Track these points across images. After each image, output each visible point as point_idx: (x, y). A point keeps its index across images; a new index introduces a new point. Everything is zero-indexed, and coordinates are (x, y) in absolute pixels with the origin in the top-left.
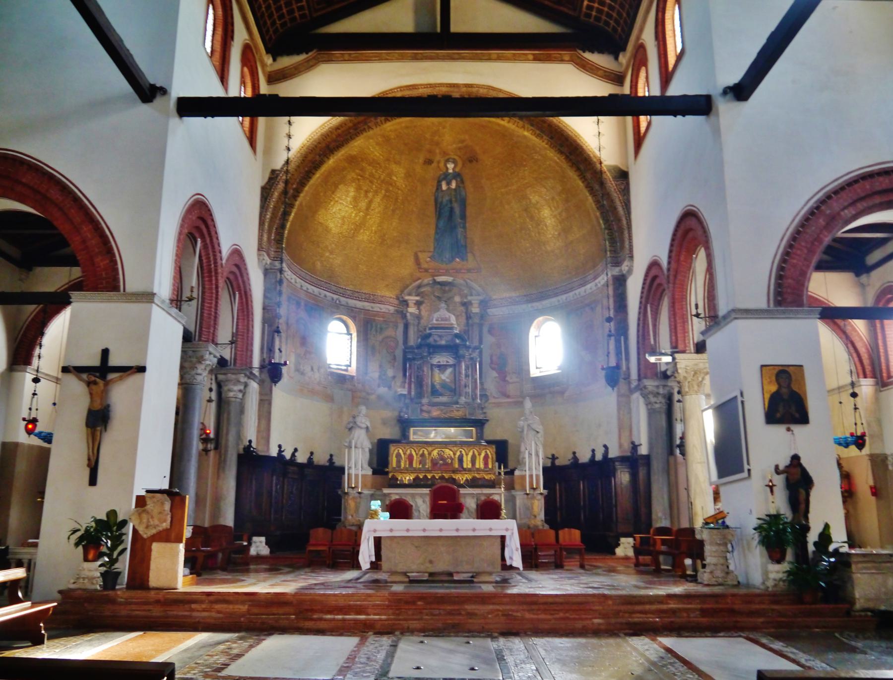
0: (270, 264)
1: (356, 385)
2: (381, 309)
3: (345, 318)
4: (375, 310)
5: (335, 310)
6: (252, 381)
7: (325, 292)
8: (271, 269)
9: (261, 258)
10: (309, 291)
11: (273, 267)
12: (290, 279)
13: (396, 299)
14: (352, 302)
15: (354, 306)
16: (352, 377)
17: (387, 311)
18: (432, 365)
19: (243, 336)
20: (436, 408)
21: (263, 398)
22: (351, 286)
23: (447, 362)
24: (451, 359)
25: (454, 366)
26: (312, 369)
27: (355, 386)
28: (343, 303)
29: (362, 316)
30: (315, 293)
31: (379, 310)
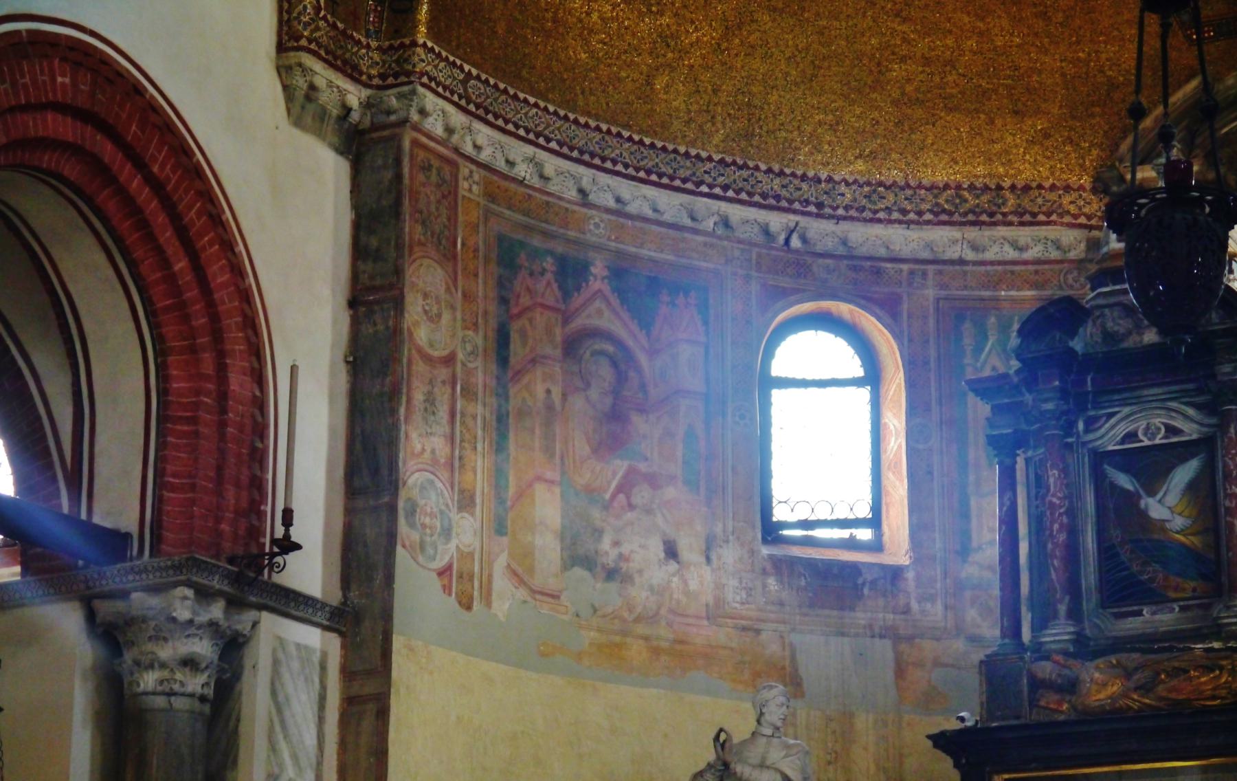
0: (367, 105)
1: (915, 606)
2: (1021, 249)
3: (844, 309)
4: (989, 255)
5: (785, 282)
6: (267, 618)
7: (723, 206)
8: (375, 127)
9: (300, 82)
10: (632, 209)
11: (382, 118)
12: (501, 165)
13: (1094, 191)
14: (865, 236)
15: (883, 252)
16: (895, 573)
17: (1054, 254)
18: (1100, 458)
19: (193, 420)
20: (1100, 662)
21: (356, 689)
22: (860, 165)
23: (1171, 430)
24: (1191, 411)
25: (1205, 446)
26: (671, 552)
27: (907, 611)
28: (829, 244)
29: (931, 293)
30: (667, 217)
31: (1011, 254)
